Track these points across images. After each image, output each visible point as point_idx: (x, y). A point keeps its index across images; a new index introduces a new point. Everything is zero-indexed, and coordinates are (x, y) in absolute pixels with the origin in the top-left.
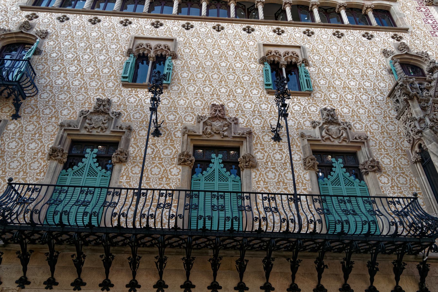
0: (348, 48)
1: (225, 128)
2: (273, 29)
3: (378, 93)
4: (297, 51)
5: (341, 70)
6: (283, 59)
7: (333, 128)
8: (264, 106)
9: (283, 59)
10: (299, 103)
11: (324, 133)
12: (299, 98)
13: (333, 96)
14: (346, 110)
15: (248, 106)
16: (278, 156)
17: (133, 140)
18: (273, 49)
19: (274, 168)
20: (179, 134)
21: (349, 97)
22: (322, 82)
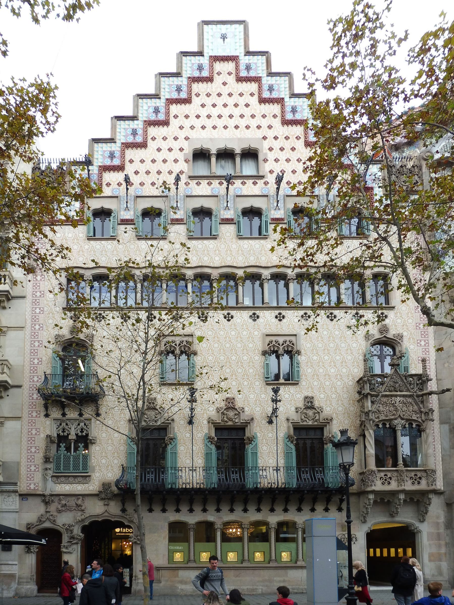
0: (337, 333)
1: (236, 417)
2: (275, 314)
3: (351, 378)
4: (293, 338)
5: (326, 358)
6: (281, 348)
7: (310, 413)
8: (263, 396)
9: (281, 348)
10: (289, 391)
11: (303, 417)
12: (290, 386)
13: (315, 383)
14: (322, 396)
15: (252, 396)
16: (270, 435)
17: (176, 428)
18: (274, 338)
19: (267, 443)
20: (205, 422)
21: (327, 383)
22: (309, 370)
